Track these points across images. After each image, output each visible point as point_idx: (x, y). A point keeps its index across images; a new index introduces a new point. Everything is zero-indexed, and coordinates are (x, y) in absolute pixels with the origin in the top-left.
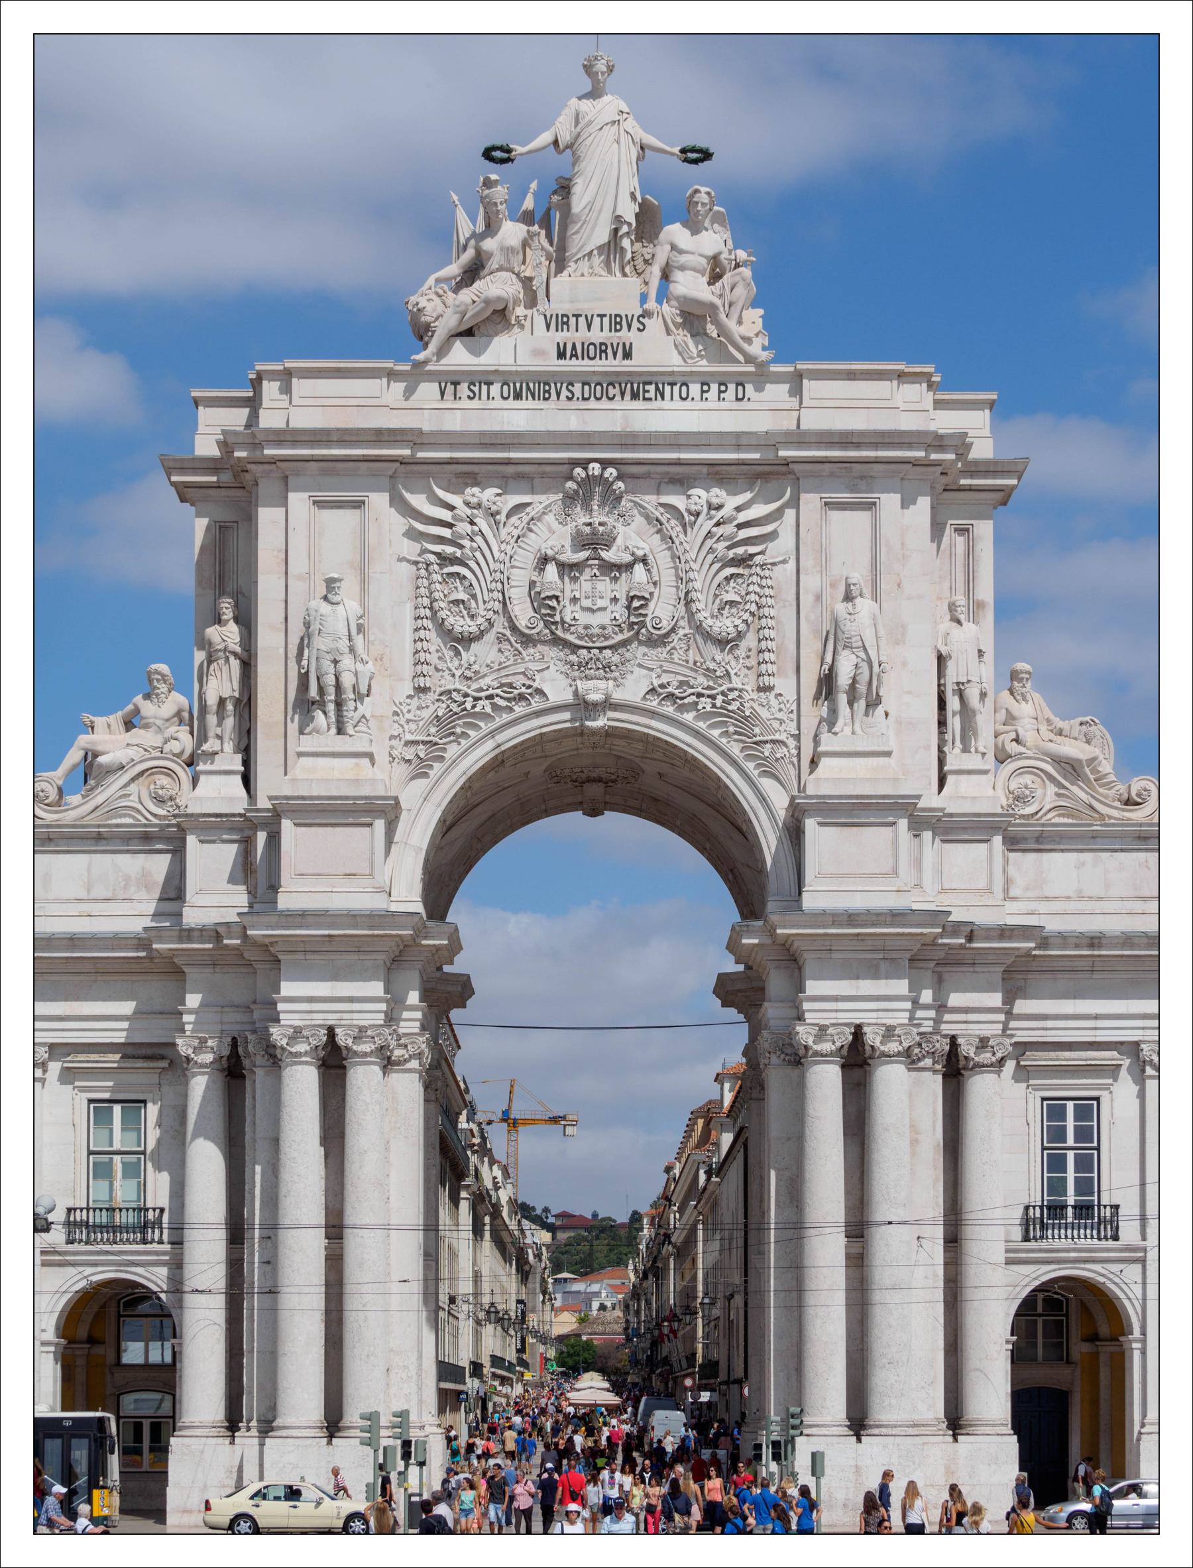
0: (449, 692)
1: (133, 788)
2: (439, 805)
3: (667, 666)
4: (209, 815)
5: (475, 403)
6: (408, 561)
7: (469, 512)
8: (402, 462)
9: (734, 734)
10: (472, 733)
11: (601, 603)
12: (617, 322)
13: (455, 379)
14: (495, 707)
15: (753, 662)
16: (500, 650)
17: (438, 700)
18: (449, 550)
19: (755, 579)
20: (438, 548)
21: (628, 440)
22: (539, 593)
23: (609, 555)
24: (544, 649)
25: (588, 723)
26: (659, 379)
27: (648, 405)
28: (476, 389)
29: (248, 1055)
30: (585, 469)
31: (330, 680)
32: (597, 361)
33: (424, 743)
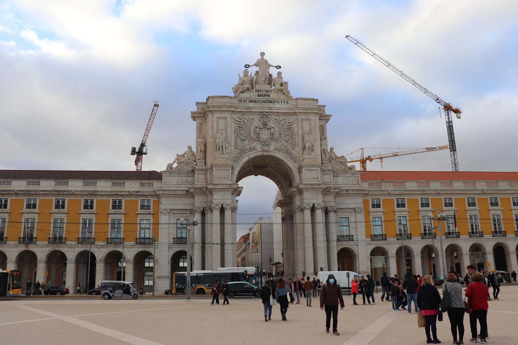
1: (185, 165)
3: (277, 145)
4: (199, 169)
5: (244, 103)
7: (243, 120)
8: (233, 111)
10: (244, 155)
11: (266, 134)
12: (267, 91)
13: (241, 99)
14: (248, 151)
18: (240, 126)
19: (291, 131)
20: (239, 126)
21: (270, 108)
22: (256, 133)
23: (267, 127)
25: (264, 154)
26: (274, 100)
27: (273, 104)
28: (244, 101)
29: (206, 210)
31: (221, 146)
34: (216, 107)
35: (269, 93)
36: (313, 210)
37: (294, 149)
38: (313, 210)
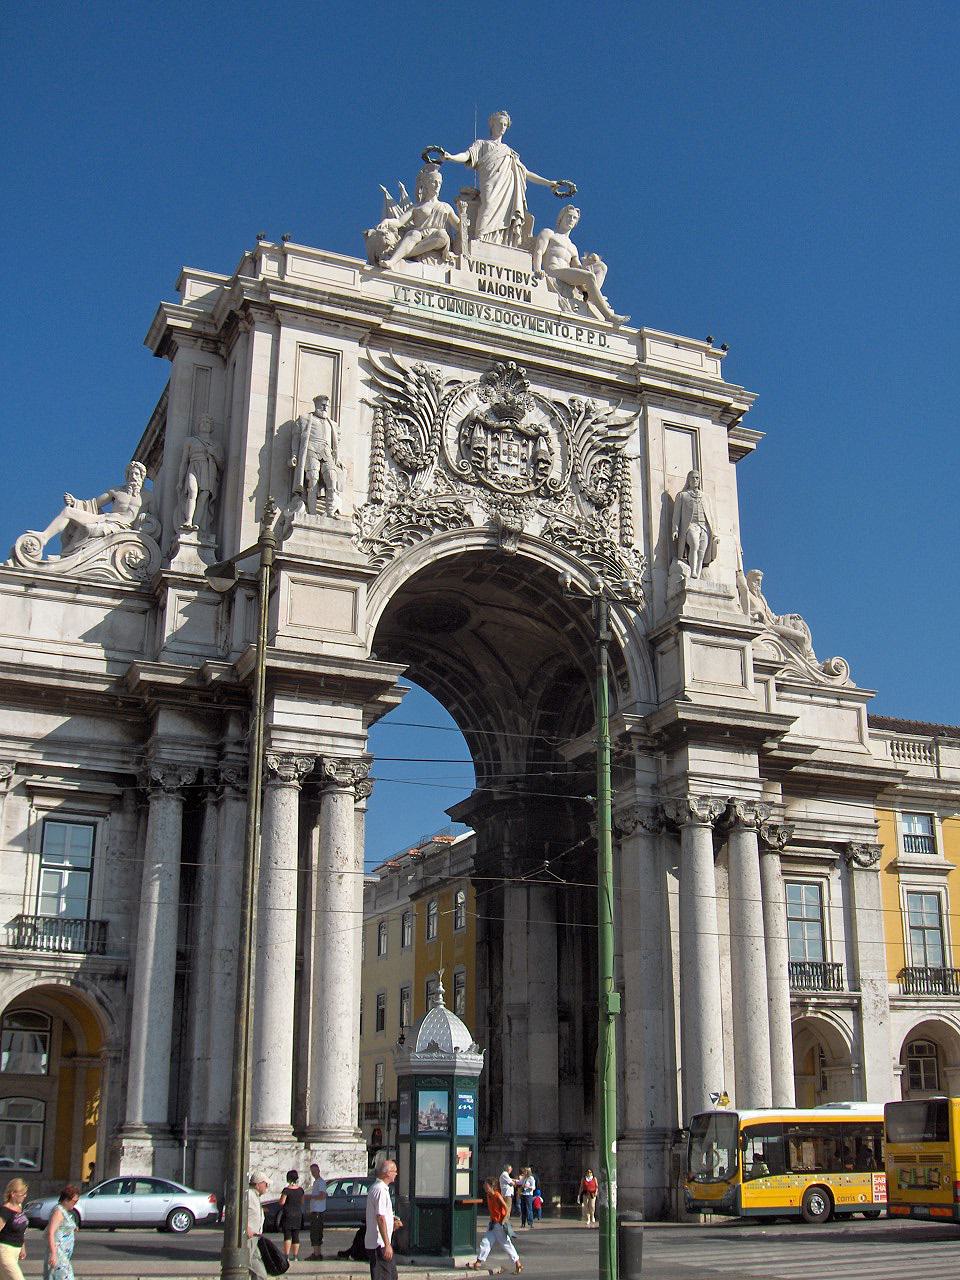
0: (399, 507)
2: (388, 593)
6: (369, 405)
7: (417, 377)
9: (609, 574)
10: (415, 541)
11: (515, 461)
12: (518, 277)
15: (617, 523)
16: (435, 482)
17: (389, 512)
20: (396, 400)
24: (470, 487)
30: (506, 364)
32: (506, 296)
33: (378, 542)
34: (297, 291)
35: (529, 287)
36: (725, 828)
37: (629, 545)
38: (725, 828)
